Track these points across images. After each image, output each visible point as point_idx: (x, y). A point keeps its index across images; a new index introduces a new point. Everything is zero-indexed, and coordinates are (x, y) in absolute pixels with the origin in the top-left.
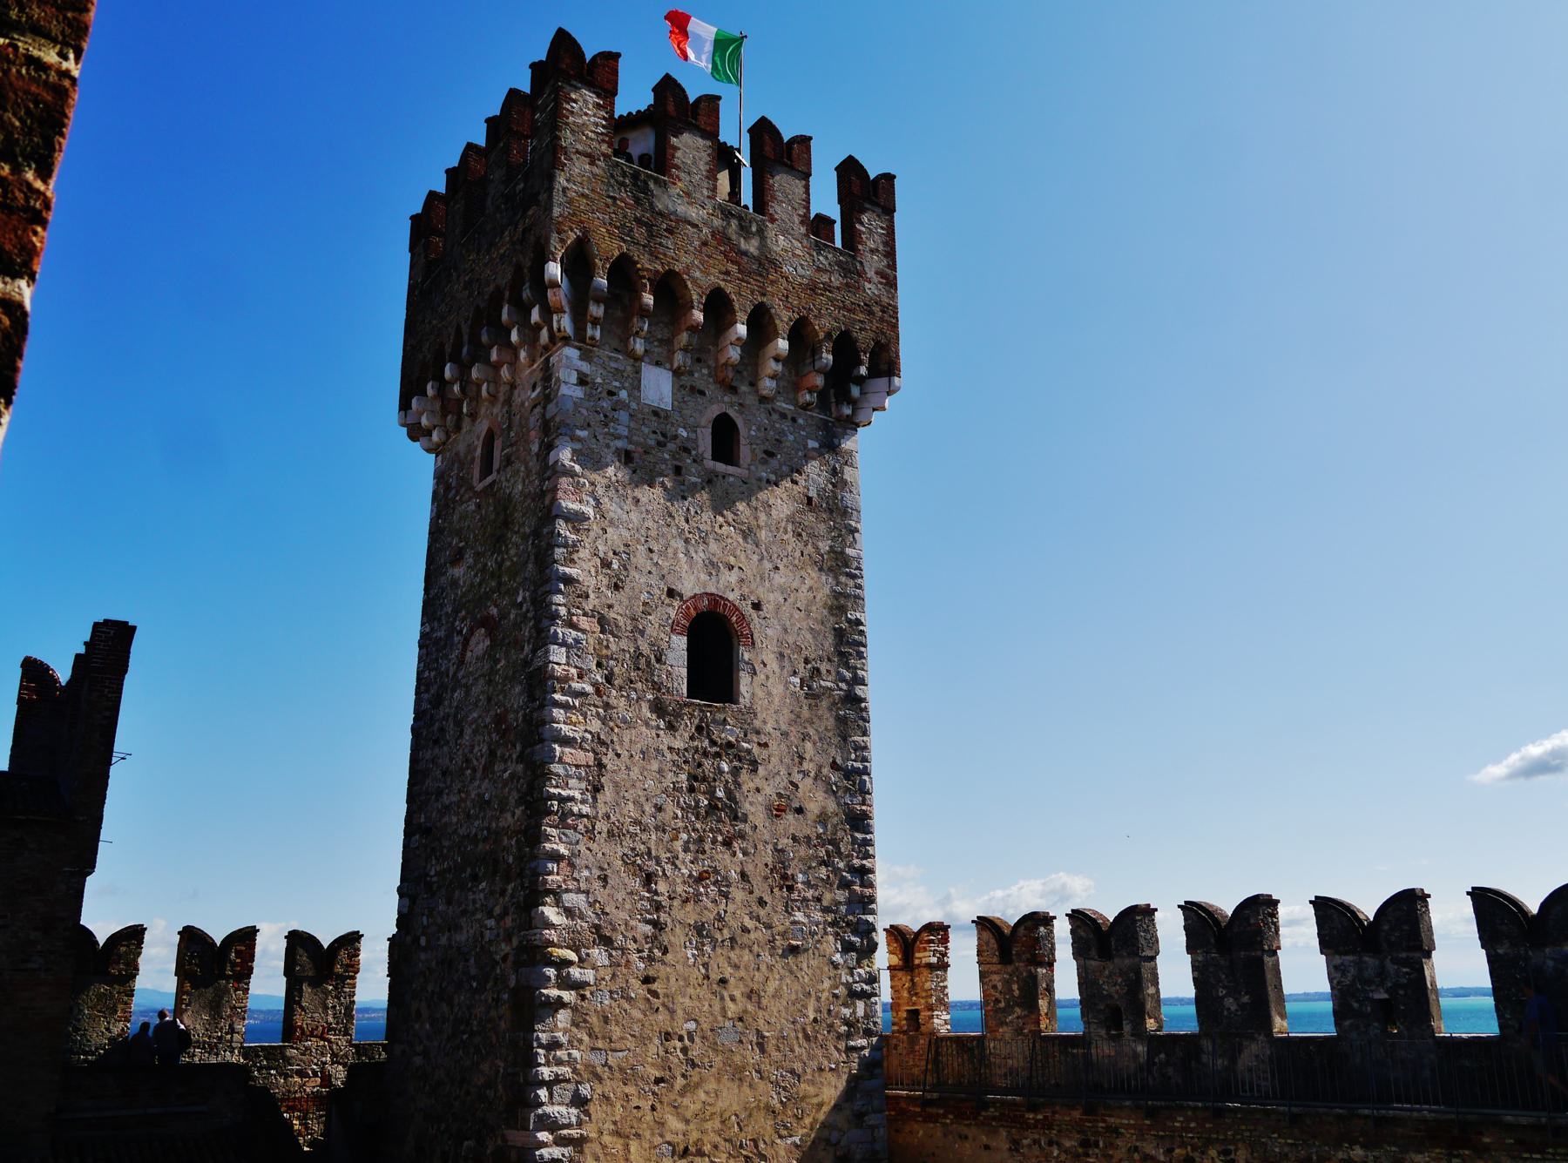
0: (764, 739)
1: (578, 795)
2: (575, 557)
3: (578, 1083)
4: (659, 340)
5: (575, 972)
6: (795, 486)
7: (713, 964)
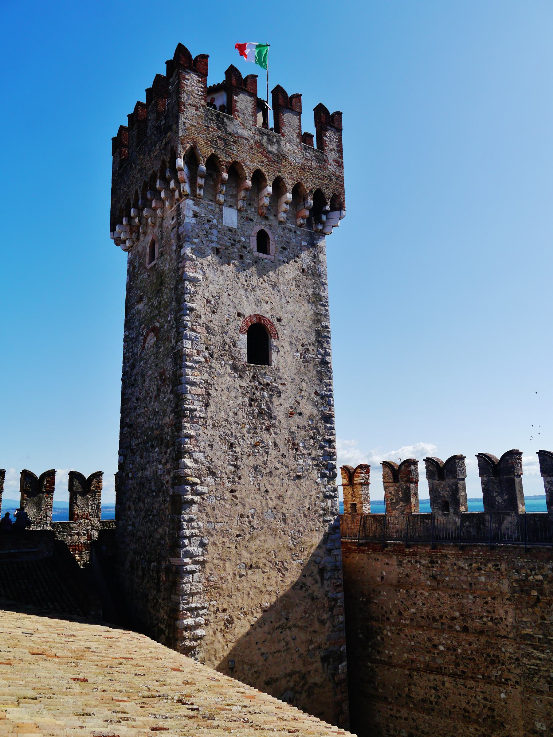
0: (283, 382)
1: (198, 408)
2: (194, 298)
3: (202, 537)
5: (199, 488)
6: (296, 264)
7: (262, 484)
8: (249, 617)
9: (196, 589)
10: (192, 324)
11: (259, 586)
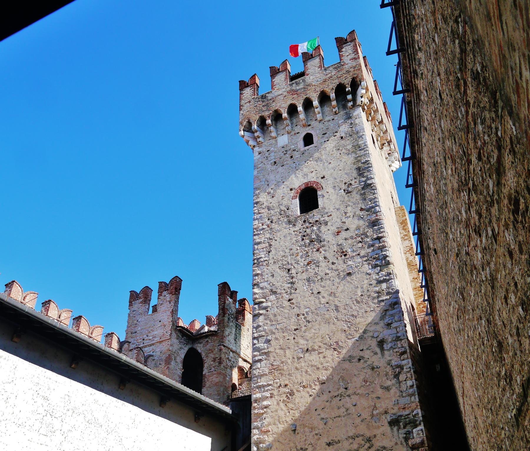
0: (329, 214)
1: (263, 256)
7: (315, 289)
8: (308, 389)
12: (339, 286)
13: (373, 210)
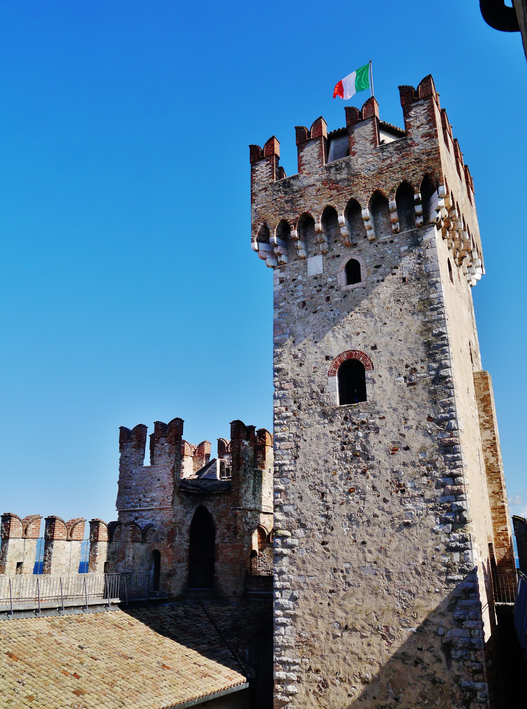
0: (382, 415)
1: (287, 462)
2: (281, 359)
3: (293, 590)
4: (314, 244)
5: (289, 541)
6: (394, 276)
7: (358, 535)
9: (287, 642)
10: (281, 384)
11: (357, 652)
12: (393, 540)
13: (447, 423)
